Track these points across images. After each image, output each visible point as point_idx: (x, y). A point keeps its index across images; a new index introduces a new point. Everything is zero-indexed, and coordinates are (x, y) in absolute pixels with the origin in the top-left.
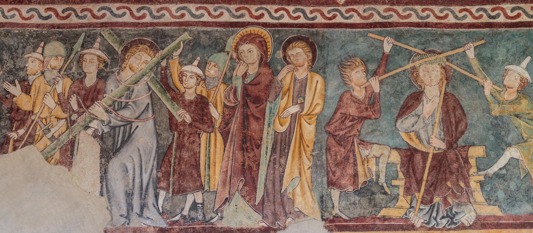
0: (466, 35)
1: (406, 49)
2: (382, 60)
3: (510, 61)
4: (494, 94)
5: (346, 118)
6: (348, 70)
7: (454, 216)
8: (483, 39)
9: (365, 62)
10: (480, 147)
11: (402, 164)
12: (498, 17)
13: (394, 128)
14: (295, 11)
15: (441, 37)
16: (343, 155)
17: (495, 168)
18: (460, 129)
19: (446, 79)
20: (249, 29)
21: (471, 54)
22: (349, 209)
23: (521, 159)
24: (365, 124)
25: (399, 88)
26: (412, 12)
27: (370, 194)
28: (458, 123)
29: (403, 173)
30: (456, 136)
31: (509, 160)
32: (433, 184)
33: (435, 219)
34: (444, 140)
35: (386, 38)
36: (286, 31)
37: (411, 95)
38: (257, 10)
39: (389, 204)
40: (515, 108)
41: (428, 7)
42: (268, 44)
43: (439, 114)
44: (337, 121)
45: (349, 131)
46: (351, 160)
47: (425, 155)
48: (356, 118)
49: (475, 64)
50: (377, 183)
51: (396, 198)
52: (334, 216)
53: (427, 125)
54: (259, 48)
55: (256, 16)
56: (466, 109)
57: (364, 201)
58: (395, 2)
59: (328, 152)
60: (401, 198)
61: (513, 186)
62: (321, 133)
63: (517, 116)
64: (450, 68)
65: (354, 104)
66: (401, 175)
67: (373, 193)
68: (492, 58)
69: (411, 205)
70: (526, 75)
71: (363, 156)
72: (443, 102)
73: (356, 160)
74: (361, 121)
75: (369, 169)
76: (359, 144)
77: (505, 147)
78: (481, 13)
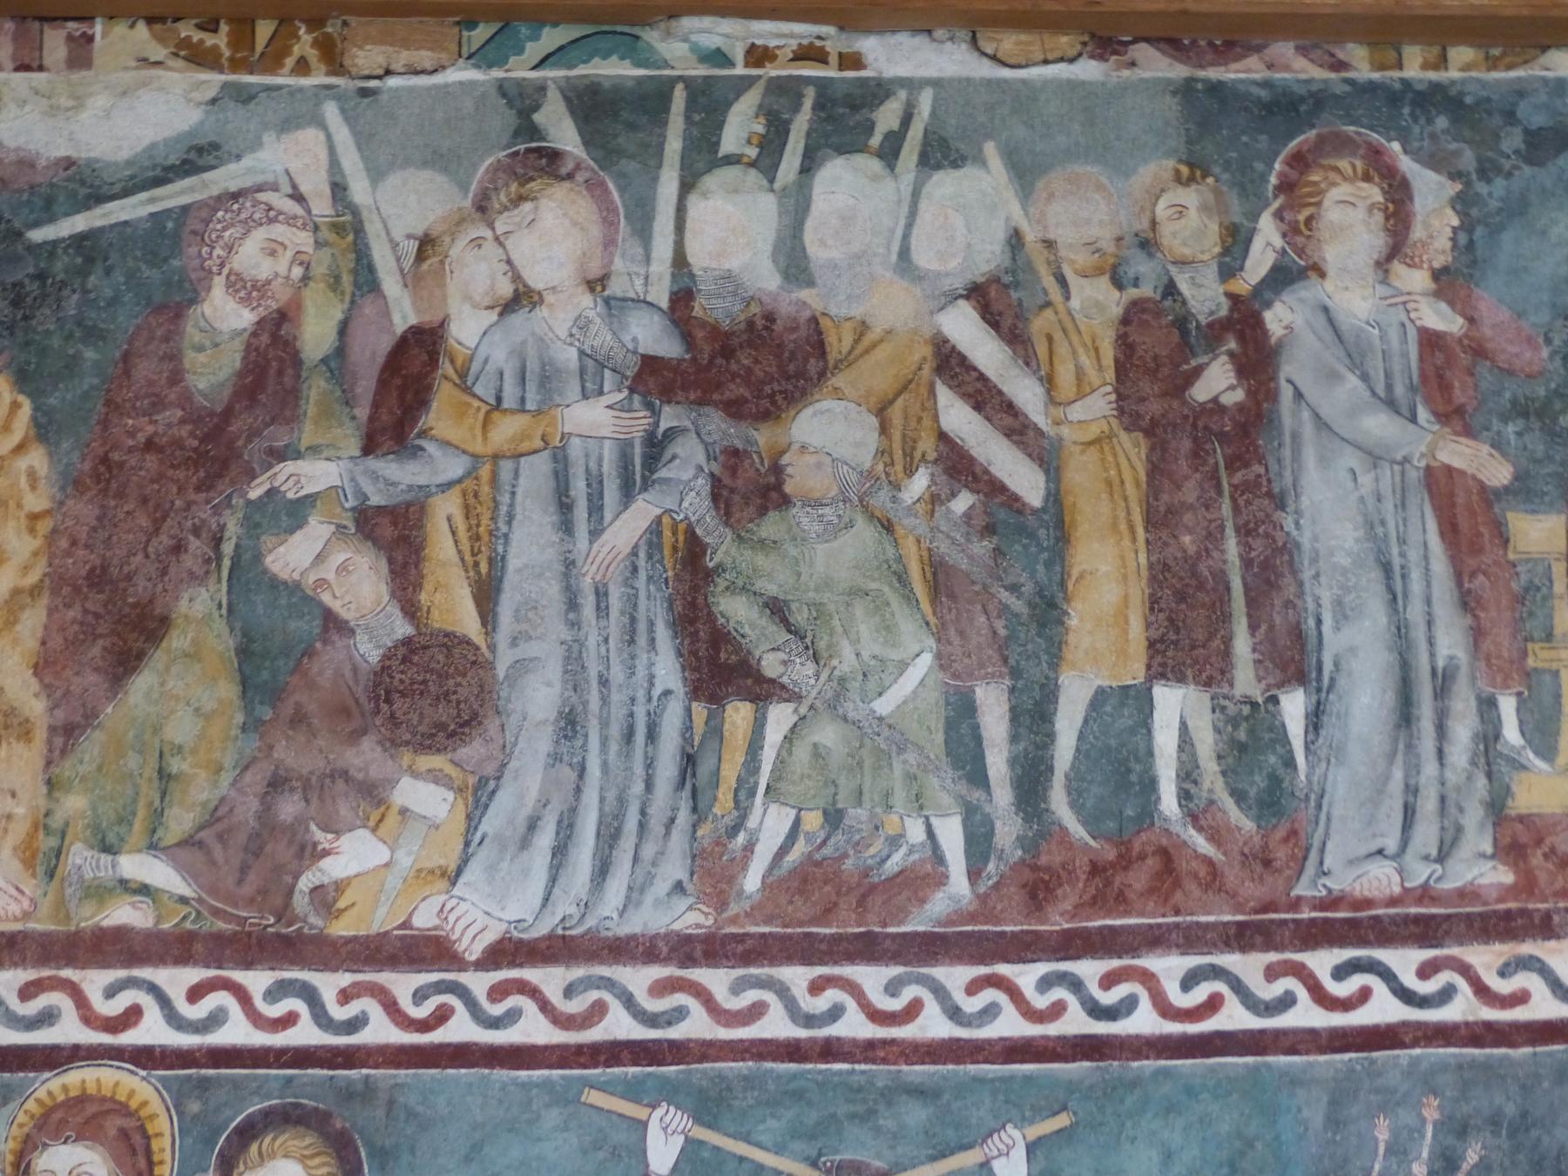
0: (994, 1093)
1: (742, 1159)
8: (1064, 1108)
12: (1129, 1012)
14: (272, 995)
15: (889, 1104)
20: (78, 1077)
26: (769, 997)
35: (659, 1112)
36: (235, 1083)
38: (111, 992)
41: (836, 970)
42: (155, 1145)
54: (118, 1160)
55: (108, 1019)
58: (698, 953)
78: (1059, 993)
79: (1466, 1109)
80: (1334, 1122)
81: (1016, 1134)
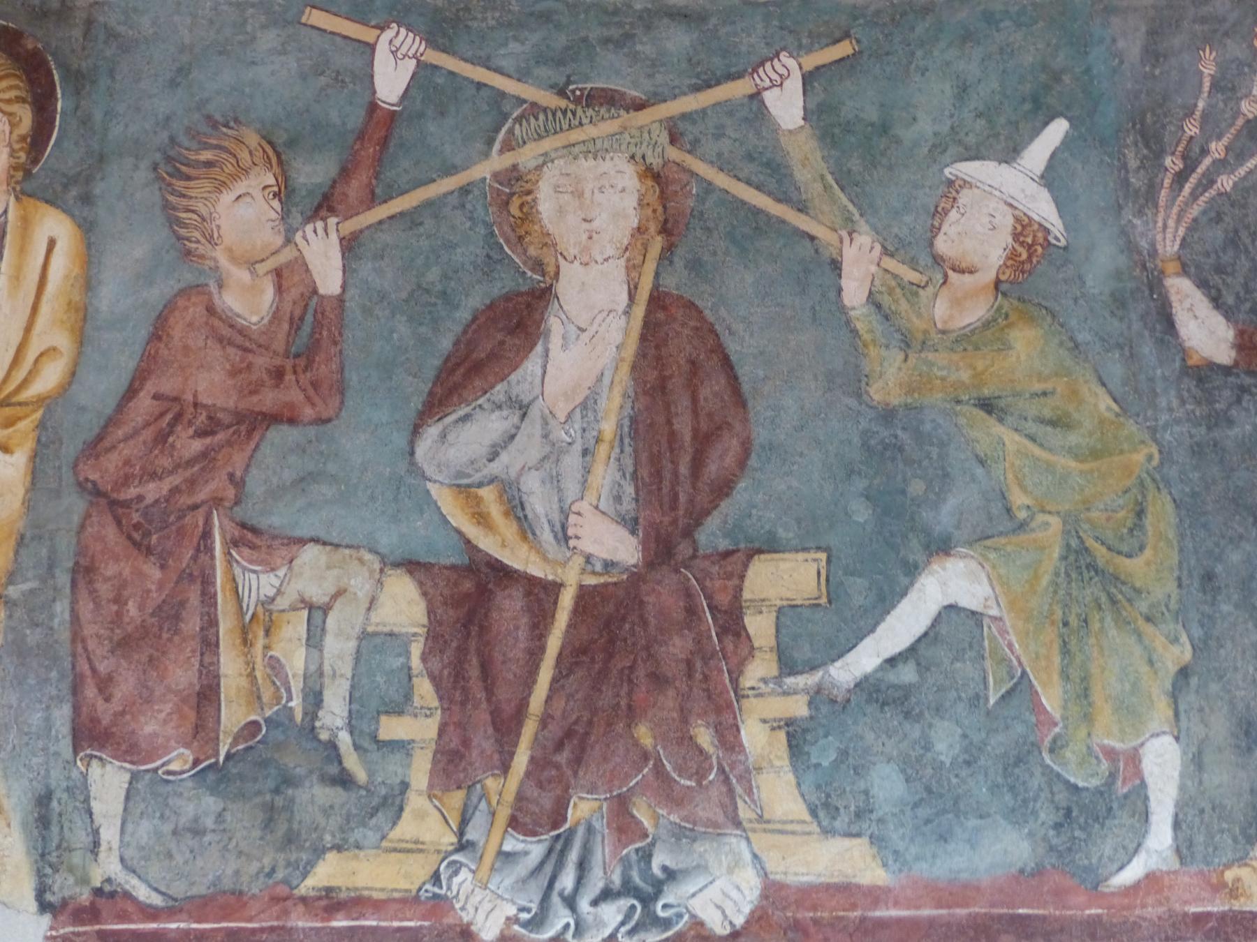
1: (480, 86)
2: (361, 136)
3: (971, 140)
4: (886, 300)
5: (178, 417)
6: (199, 188)
7: (659, 887)
8: (847, 35)
9: (279, 151)
10: (801, 556)
11: (435, 639)
13: (402, 467)
15: (648, 28)
16: (156, 598)
17: (865, 659)
18: (712, 469)
19: (665, 230)
21: (787, 106)
22: (170, 855)
23: (994, 612)
24: (266, 449)
25: (433, 275)
27: (271, 784)
28: (704, 441)
29: (435, 679)
30: (691, 501)
31: (937, 621)
32: (569, 734)
33: (570, 902)
34: (632, 525)
35: (388, 34)
37: (490, 307)
39: (357, 834)
40: (980, 365)
43: (617, 400)
44: (136, 433)
45: (192, 483)
46: (192, 623)
47: (541, 594)
48: (225, 418)
49: (807, 160)
50: (310, 731)
51: (392, 803)
52: (98, 892)
53: (562, 452)
56: (746, 372)
57: (243, 821)
59: (82, 584)
60: (416, 801)
61: (946, 742)
62: (57, 494)
63: (987, 406)
64: (684, 177)
65: (218, 353)
66: (424, 690)
67: (288, 781)
68: (884, 128)
69: (461, 833)
70: (1044, 209)
71: (250, 603)
72: (643, 338)
73: (212, 622)
74: (250, 434)
75: (275, 666)
76: (235, 543)
77: (920, 557)
80: (1153, 55)
81: (792, 63)
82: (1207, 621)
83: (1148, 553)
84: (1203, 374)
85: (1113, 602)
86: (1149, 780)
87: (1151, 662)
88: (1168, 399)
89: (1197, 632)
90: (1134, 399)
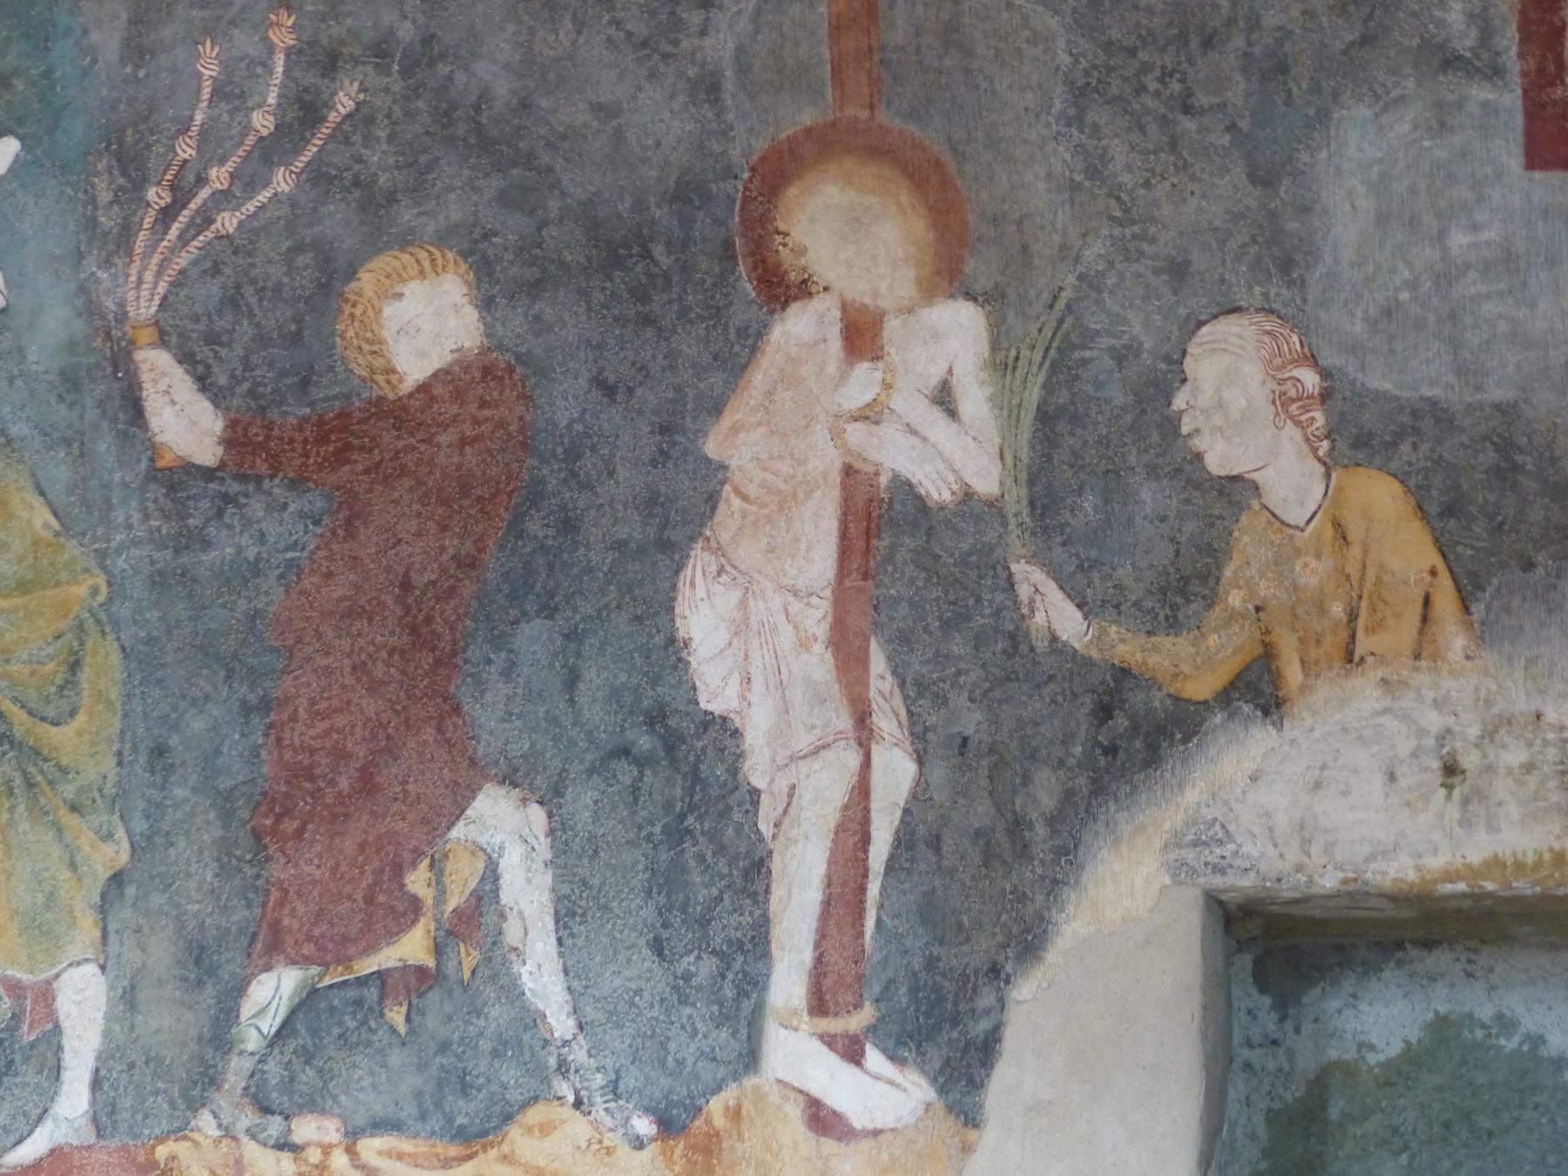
79: (336, 30)
80: (137, 51)
82: (155, 810)
83: (81, 718)
84: (176, 479)
85: (30, 785)
86: (66, 1025)
87: (73, 866)
88: (126, 512)
89: (140, 825)
90: (80, 514)
